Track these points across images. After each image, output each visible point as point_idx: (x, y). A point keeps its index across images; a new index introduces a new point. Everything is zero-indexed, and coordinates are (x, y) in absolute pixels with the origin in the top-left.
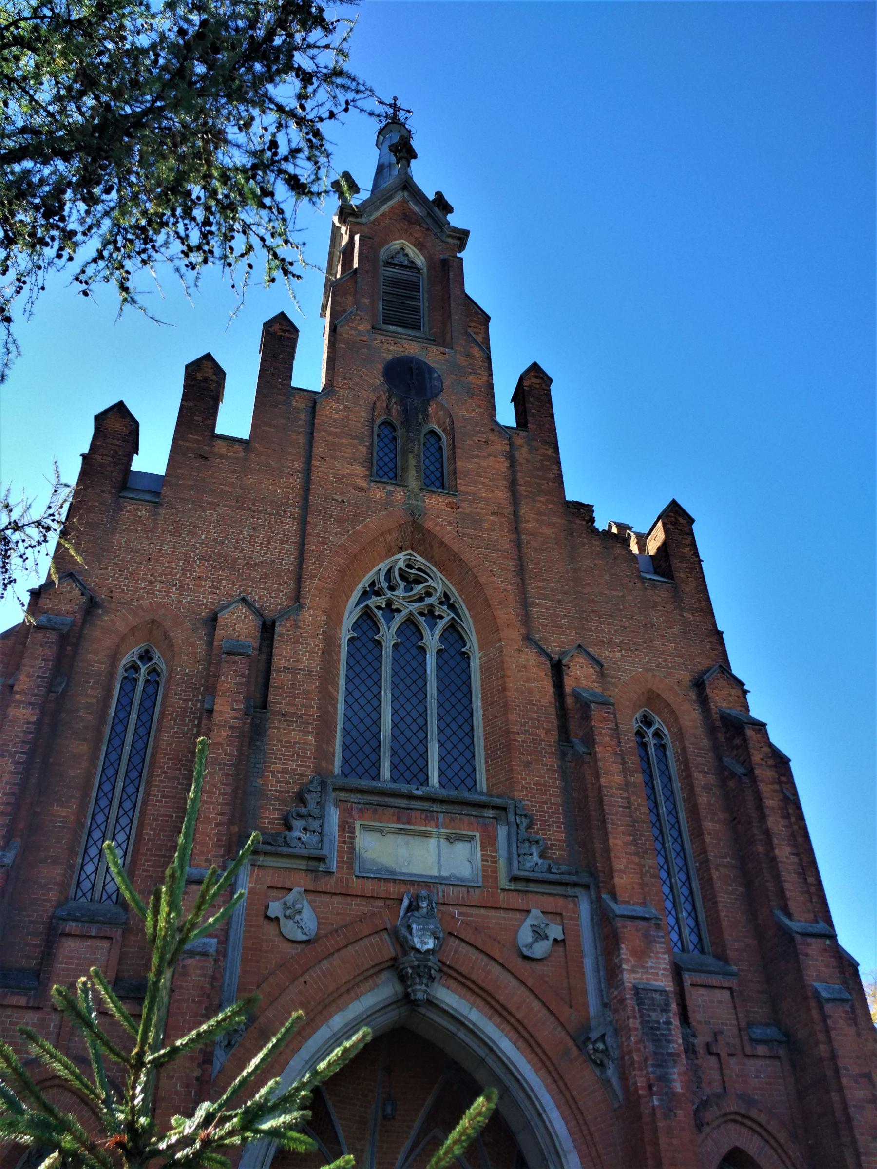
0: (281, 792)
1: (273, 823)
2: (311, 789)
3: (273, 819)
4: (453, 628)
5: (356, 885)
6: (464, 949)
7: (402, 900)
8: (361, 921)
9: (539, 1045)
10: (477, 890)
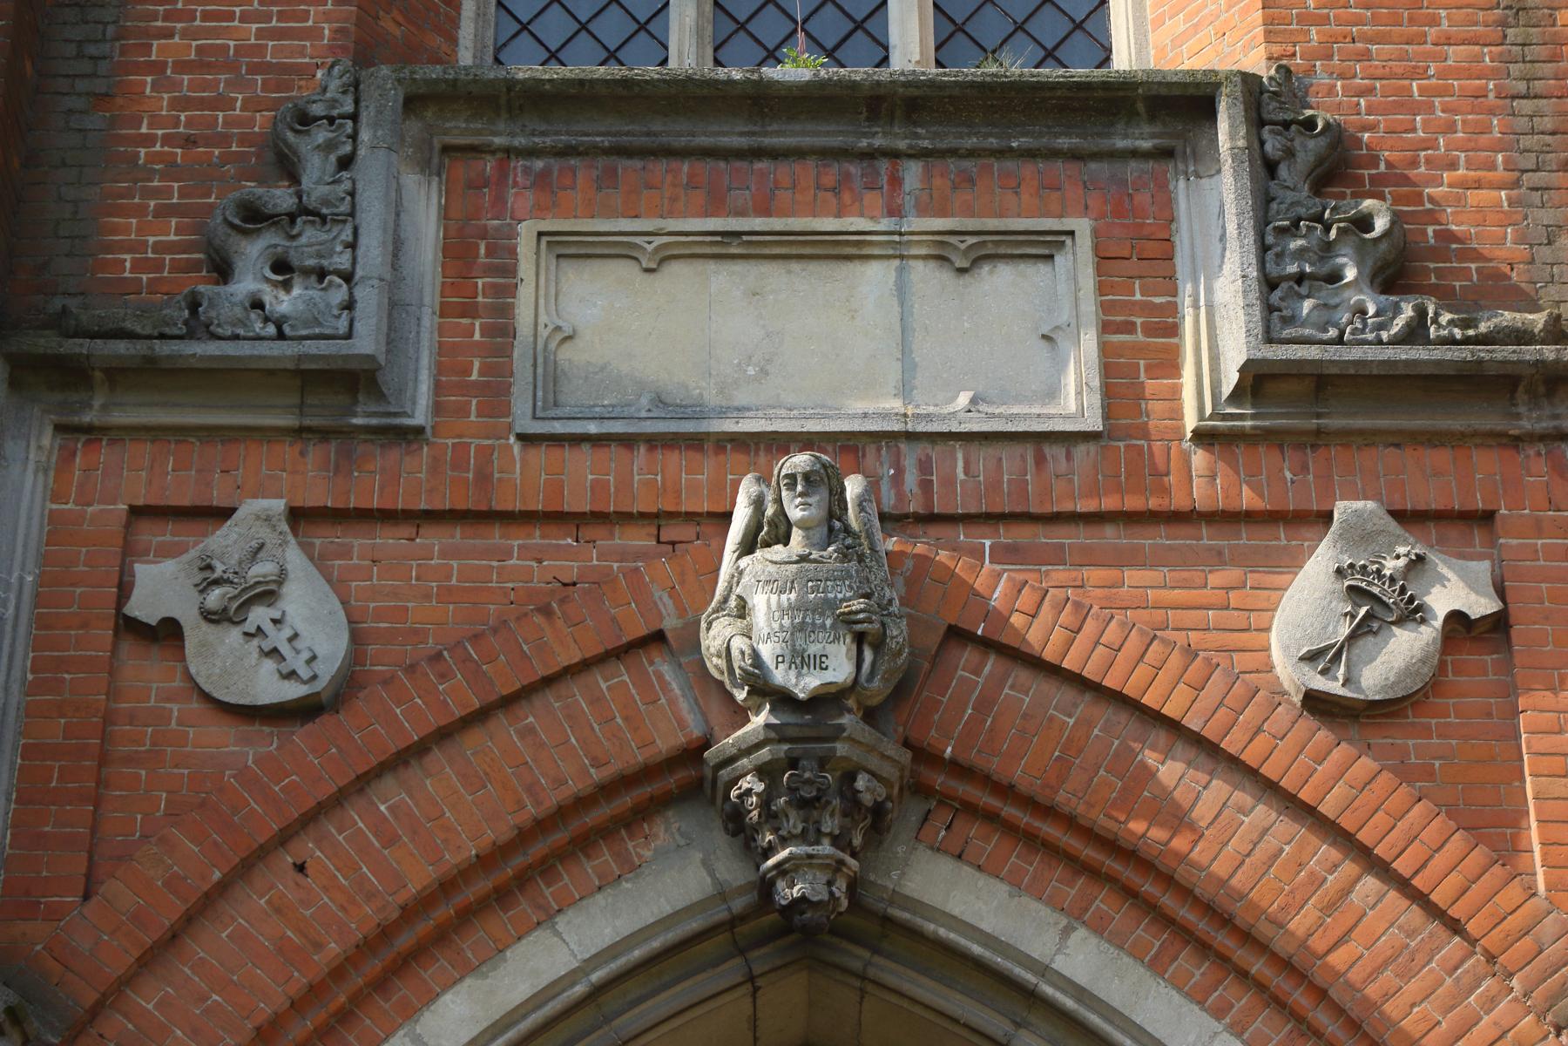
0: (189, 142)
1: (158, 266)
2: (317, 109)
3: (158, 247)
5: (523, 478)
8: (546, 611)
10: (1080, 450)
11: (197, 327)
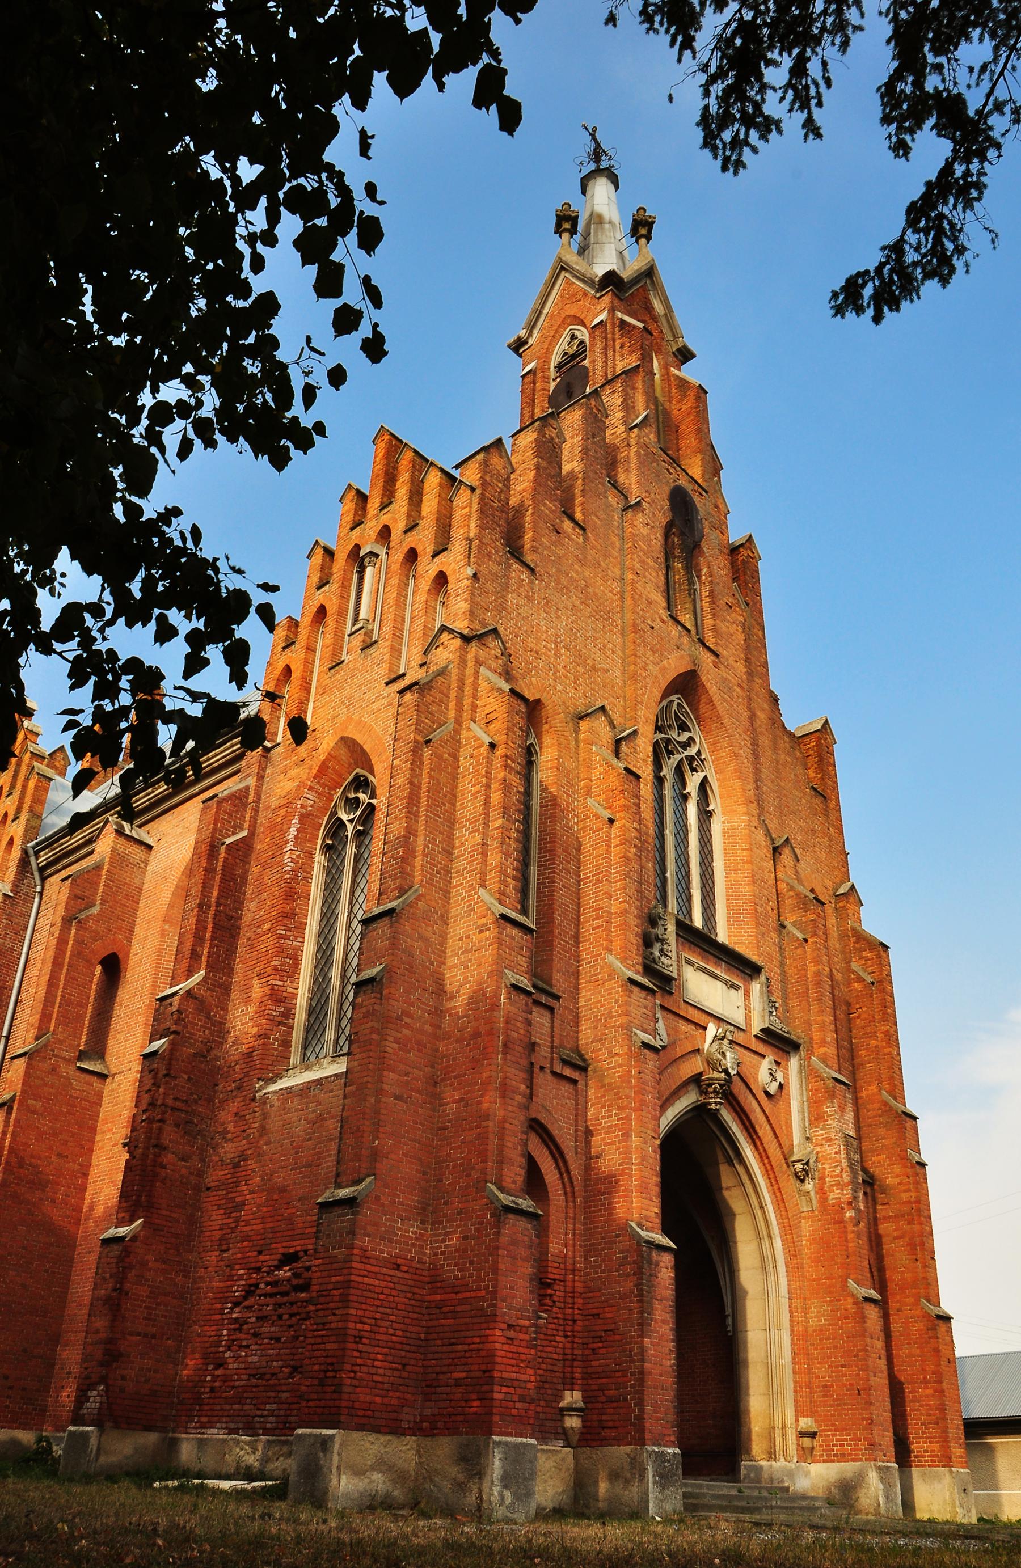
4: (704, 784)
7: (705, 1029)
9: (768, 1158)
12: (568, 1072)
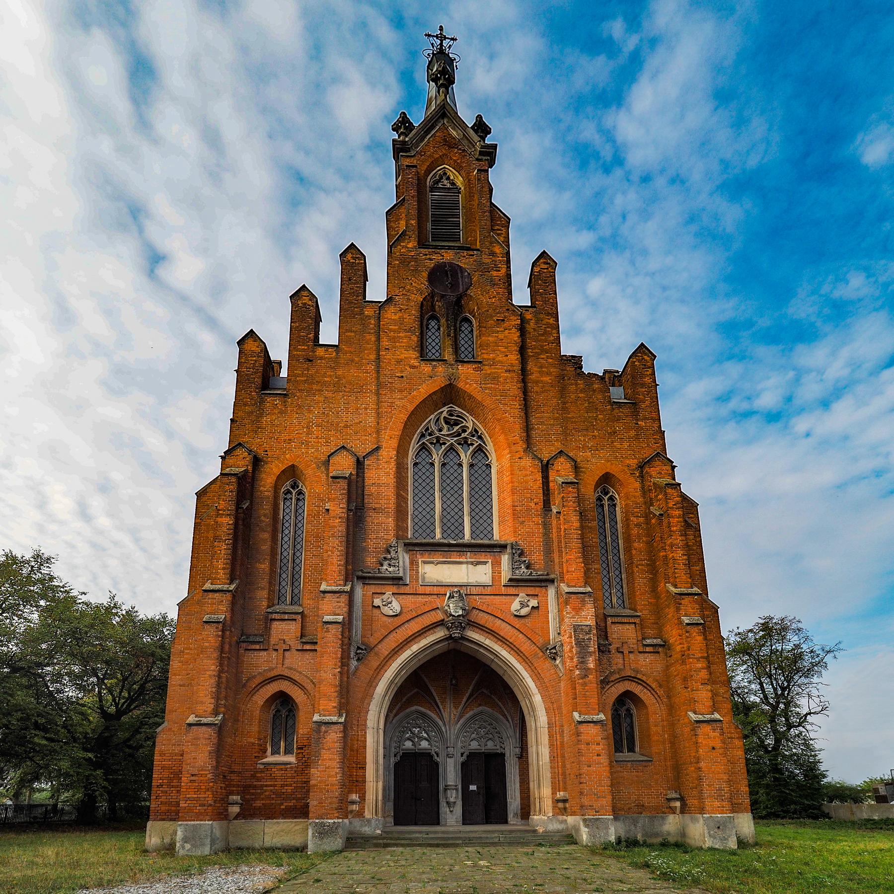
5: (421, 590)
6: (481, 614)
11: (380, 572)
12: (308, 647)
